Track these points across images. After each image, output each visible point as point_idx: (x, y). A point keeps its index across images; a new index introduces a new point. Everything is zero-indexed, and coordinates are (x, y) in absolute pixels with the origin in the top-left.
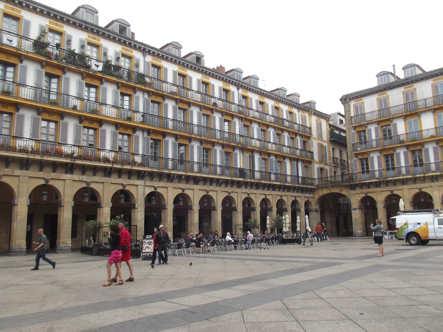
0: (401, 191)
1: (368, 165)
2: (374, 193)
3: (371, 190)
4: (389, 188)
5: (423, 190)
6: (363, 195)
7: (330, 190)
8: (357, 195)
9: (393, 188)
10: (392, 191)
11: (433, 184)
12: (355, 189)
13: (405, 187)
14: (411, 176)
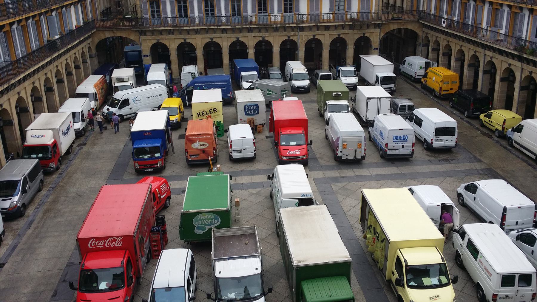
0: (194, 40)
1: (159, 8)
2: (166, 40)
3: (163, 37)
4: (182, 36)
5: (214, 40)
6: (154, 42)
7: (114, 33)
8: (148, 41)
9: (187, 37)
10: (185, 39)
11: (223, 35)
12: (145, 35)
13: (198, 36)
14: (206, 28)
